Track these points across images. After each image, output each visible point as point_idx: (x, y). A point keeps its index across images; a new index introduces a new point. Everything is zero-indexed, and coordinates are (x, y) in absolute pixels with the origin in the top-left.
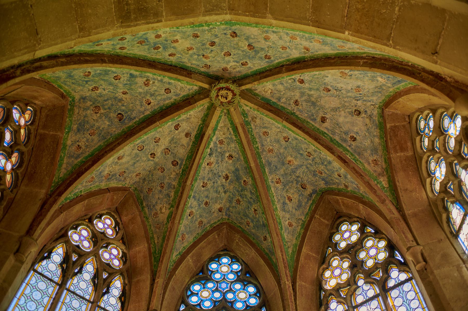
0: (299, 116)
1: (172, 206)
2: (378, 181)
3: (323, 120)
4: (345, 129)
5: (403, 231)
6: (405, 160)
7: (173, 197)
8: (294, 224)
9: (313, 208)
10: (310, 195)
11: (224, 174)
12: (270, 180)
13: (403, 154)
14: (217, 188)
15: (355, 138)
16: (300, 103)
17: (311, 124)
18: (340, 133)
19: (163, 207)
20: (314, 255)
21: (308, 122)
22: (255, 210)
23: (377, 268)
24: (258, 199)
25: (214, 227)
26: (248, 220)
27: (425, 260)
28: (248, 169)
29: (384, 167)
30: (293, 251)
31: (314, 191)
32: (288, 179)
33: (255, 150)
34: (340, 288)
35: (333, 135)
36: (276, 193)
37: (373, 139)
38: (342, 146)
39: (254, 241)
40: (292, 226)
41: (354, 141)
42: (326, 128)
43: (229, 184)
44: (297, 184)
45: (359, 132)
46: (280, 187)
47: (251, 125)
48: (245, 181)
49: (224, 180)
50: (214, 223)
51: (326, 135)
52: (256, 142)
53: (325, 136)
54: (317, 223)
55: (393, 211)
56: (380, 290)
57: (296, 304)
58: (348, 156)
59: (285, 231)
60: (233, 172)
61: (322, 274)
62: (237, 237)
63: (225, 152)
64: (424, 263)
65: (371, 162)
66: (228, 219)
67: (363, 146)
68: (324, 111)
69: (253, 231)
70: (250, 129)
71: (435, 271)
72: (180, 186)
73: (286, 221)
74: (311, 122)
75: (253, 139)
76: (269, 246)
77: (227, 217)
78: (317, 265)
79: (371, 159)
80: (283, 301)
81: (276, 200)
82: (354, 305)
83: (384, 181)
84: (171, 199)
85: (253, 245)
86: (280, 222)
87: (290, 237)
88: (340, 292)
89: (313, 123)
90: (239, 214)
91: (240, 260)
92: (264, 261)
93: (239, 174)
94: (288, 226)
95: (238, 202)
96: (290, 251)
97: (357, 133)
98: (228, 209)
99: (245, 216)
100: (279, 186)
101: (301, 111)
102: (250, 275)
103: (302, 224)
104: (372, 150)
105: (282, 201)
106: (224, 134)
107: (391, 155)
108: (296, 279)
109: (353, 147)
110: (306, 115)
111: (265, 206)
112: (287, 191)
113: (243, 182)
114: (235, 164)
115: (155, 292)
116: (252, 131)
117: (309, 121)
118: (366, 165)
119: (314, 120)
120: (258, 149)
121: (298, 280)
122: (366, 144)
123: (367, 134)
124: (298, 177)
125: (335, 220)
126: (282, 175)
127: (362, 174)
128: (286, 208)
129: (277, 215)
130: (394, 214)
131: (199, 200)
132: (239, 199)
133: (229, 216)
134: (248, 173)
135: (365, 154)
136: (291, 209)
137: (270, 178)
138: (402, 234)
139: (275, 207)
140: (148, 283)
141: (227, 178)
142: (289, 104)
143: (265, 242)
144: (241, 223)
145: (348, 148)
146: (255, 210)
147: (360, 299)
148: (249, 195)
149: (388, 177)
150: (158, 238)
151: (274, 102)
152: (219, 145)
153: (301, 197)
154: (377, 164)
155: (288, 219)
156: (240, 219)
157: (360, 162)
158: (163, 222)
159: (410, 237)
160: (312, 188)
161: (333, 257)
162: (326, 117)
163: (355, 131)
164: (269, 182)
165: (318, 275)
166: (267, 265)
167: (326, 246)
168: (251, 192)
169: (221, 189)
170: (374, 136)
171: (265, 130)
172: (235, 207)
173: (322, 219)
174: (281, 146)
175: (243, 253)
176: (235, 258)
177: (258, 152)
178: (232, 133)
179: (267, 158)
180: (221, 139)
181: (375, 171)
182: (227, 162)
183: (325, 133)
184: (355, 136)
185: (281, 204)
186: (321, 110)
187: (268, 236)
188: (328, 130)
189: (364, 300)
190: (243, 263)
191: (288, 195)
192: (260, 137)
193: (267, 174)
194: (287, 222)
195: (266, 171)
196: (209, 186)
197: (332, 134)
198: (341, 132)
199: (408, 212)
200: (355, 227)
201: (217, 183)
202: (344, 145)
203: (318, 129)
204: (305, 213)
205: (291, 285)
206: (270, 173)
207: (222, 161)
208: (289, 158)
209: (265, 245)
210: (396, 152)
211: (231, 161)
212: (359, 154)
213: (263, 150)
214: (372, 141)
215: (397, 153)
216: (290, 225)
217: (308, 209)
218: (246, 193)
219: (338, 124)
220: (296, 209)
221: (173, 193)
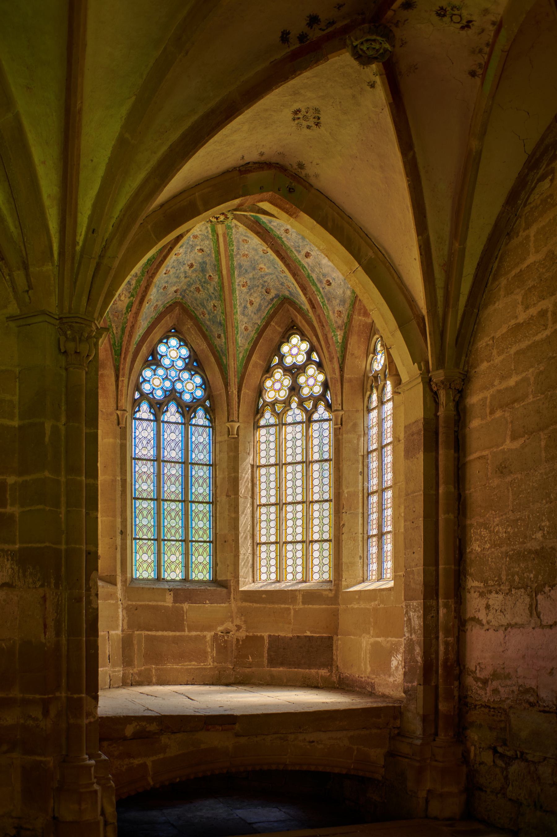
0: (285, 242)
1: (132, 296)
2: (335, 334)
3: (307, 255)
4: (324, 271)
5: (336, 393)
6: (363, 325)
7: (134, 285)
8: (250, 328)
9: (271, 312)
10: (272, 300)
11: (189, 263)
12: (237, 283)
13: (364, 319)
14: (178, 274)
15: (331, 283)
16: (290, 233)
17: (295, 254)
18: (318, 272)
19: (123, 294)
20: (261, 362)
21: (292, 251)
22: (214, 306)
23: (310, 399)
24: (221, 297)
25: (167, 308)
26: (205, 310)
27: (341, 424)
28: (217, 267)
29: (345, 321)
30: (243, 356)
31: (277, 296)
32: (255, 283)
33: (230, 252)
34: (276, 403)
35: (312, 272)
36: (240, 297)
37: (345, 290)
38: (316, 285)
39: (207, 333)
40: (248, 330)
41: (328, 285)
42: (307, 263)
43: (192, 272)
44: (262, 288)
45: (336, 279)
46: (245, 290)
47: (232, 230)
48: (210, 276)
49: (188, 268)
50: (167, 303)
51: (305, 269)
52: (233, 245)
53: (304, 270)
54: (271, 331)
55: (336, 371)
56: (306, 419)
57: (238, 411)
58: (318, 298)
59: (240, 335)
60: (200, 263)
61: (264, 382)
62: (189, 324)
63: (196, 245)
64: (340, 426)
65: (336, 312)
66: (182, 299)
67: (335, 293)
68: (310, 248)
69: (207, 322)
70: (230, 233)
71: (344, 435)
72: (143, 276)
73: (242, 325)
74: (295, 252)
75: (231, 241)
76: (222, 345)
77: (181, 297)
78: (262, 372)
79: (337, 309)
80: (228, 405)
81: (238, 304)
82: (284, 422)
83: (339, 336)
84: (132, 287)
85: (205, 337)
86: (238, 326)
87: (244, 341)
88: (276, 406)
89: (297, 254)
90: (196, 300)
91: (189, 345)
92: (215, 359)
93: (206, 267)
94: (244, 330)
95: (198, 290)
96: (241, 356)
97: (334, 279)
98: (185, 291)
99: (203, 306)
100: (245, 289)
101: (288, 239)
102: (197, 363)
103: (257, 328)
104: (341, 301)
105: (243, 305)
106: (201, 231)
107: (354, 316)
108: (242, 387)
109: (326, 290)
110: (292, 244)
111: (228, 314)
112: (251, 295)
113: (208, 276)
114: (204, 257)
115: (121, 391)
116: (231, 235)
117: (293, 250)
118: (331, 313)
119: (299, 252)
120: (233, 251)
121: (243, 388)
122: (338, 292)
123: (342, 283)
124: (265, 282)
125: (288, 329)
126: (250, 279)
127: (324, 324)
128: (246, 312)
129: (236, 319)
130: (335, 374)
131: (158, 287)
132: (199, 288)
133: (184, 297)
134: (216, 270)
135: (334, 302)
136: (250, 313)
137: (238, 280)
138: (335, 396)
139: (235, 311)
140: (113, 379)
141: (191, 266)
142: (279, 229)
143: (218, 339)
144: (197, 310)
145: (321, 289)
146: (214, 306)
147: (289, 420)
148: (212, 290)
149: (345, 333)
150: (117, 328)
151: (263, 222)
152: (192, 239)
153: (262, 301)
154: (340, 316)
155: (246, 323)
156: (195, 305)
157: (327, 308)
158: (122, 311)
159: (339, 402)
160: (276, 292)
161: (278, 368)
162: (310, 253)
163: (333, 276)
164: (235, 285)
165: (260, 382)
166: (217, 365)
167: (273, 354)
168: (214, 288)
169: (182, 275)
170: (348, 288)
171: (246, 238)
172: (193, 292)
173: (276, 327)
174: (258, 254)
175: (193, 341)
176: (184, 341)
177: (232, 255)
178: (210, 232)
179: (239, 261)
180: (196, 234)
181: (336, 322)
182: (196, 253)
183: (305, 267)
184: (331, 281)
185: (242, 308)
186: (309, 246)
187: (222, 335)
188: (309, 265)
189: (293, 422)
190: (191, 350)
191: (251, 299)
192: (238, 242)
193: (236, 276)
194: (244, 326)
195: (236, 273)
196: (171, 273)
197: (311, 270)
198: (320, 272)
199: (346, 376)
200: (305, 346)
201: (180, 270)
202: (319, 285)
203: (300, 261)
204: (262, 317)
205: (237, 394)
206: (239, 276)
207: (191, 251)
208: (262, 266)
209: (217, 342)
210: (359, 314)
211: (200, 254)
212: (328, 300)
213: (238, 253)
214: (344, 292)
215: (360, 316)
216: (246, 329)
217: (266, 313)
218: (208, 287)
219: (319, 265)
220: (255, 313)
221: (135, 281)
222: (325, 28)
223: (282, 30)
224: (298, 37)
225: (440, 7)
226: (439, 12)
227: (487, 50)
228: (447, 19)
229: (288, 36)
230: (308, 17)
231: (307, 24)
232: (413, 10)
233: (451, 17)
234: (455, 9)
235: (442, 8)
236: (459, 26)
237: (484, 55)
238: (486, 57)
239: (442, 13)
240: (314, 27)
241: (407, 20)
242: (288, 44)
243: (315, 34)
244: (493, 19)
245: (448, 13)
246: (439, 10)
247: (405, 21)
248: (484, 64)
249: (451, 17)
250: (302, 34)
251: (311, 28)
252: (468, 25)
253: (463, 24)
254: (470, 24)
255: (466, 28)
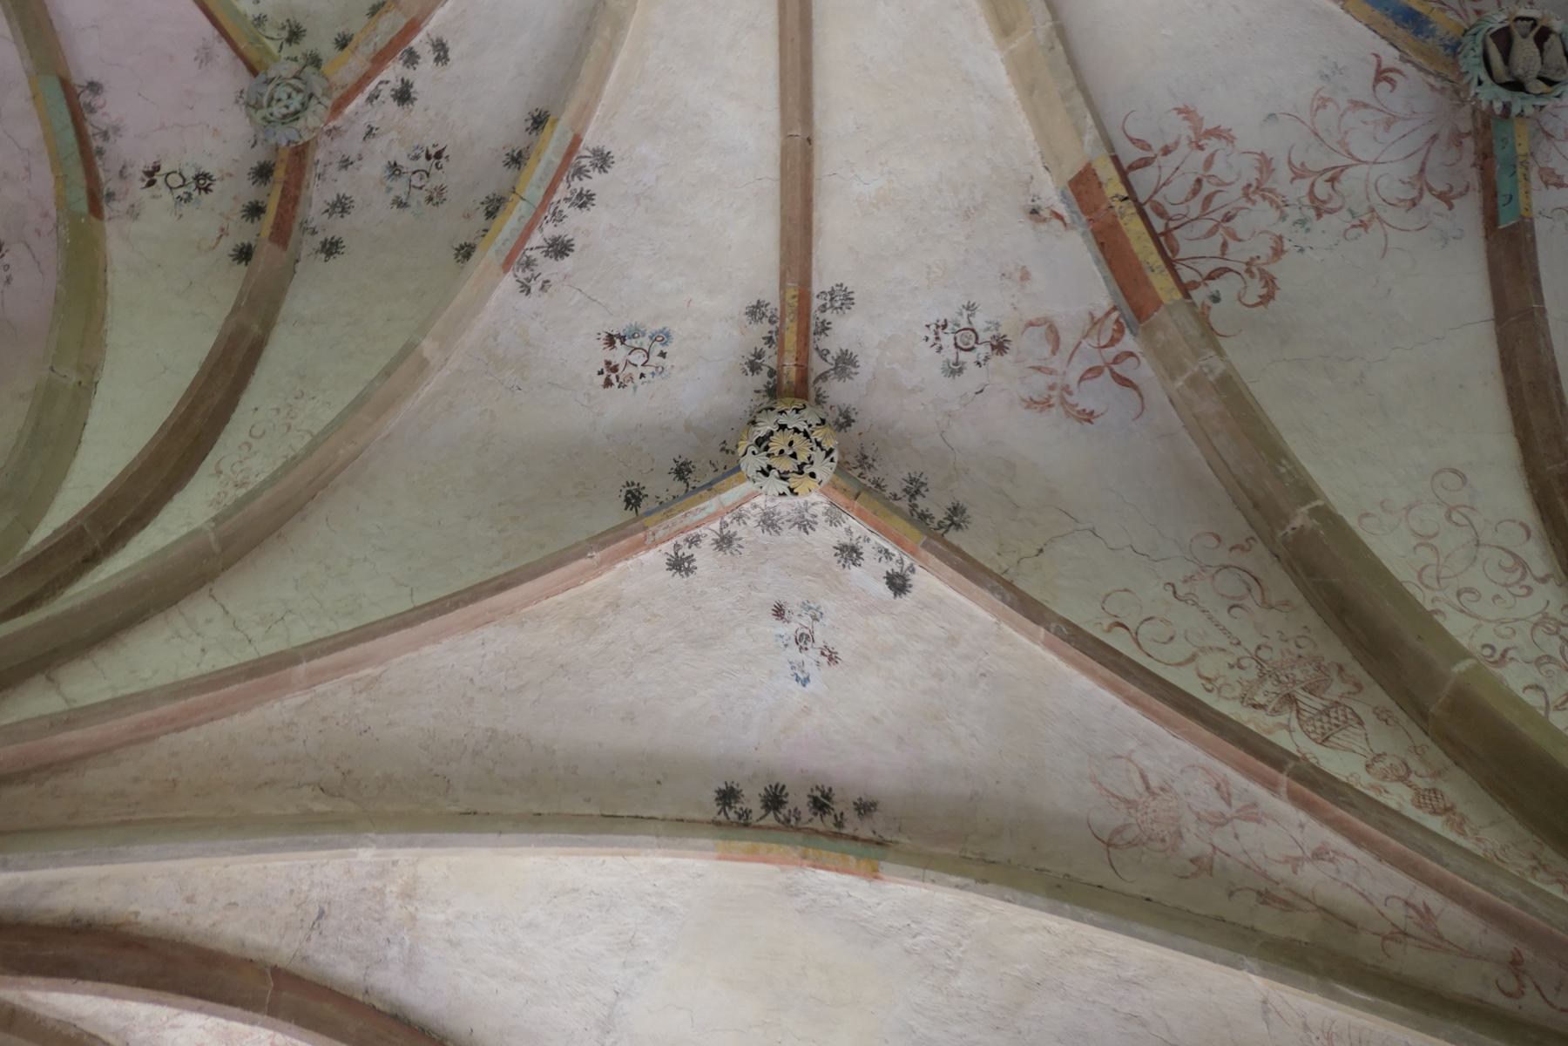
222: (381, 87)
223: (449, 63)
224: (418, 57)
225: (211, 191)
226: (208, 182)
227: (96, 143)
228: (190, 174)
229: (436, 54)
230: (415, 99)
231: (411, 86)
232: (252, 168)
233: (184, 180)
234: (185, 196)
235: (207, 190)
236: (165, 169)
237: (96, 131)
238: (90, 130)
239: (201, 182)
240: (399, 83)
241: (253, 146)
242: (432, 40)
243: (393, 72)
244: (114, 205)
245: (193, 186)
246: (209, 185)
247: (256, 142)
248: (86, 115)
249: (184, 180)
250: (415, 65)
251: (403, 80)
252: (151, 175)
253: (160, 175)
254: (147, 179)
255: (150, 169)
